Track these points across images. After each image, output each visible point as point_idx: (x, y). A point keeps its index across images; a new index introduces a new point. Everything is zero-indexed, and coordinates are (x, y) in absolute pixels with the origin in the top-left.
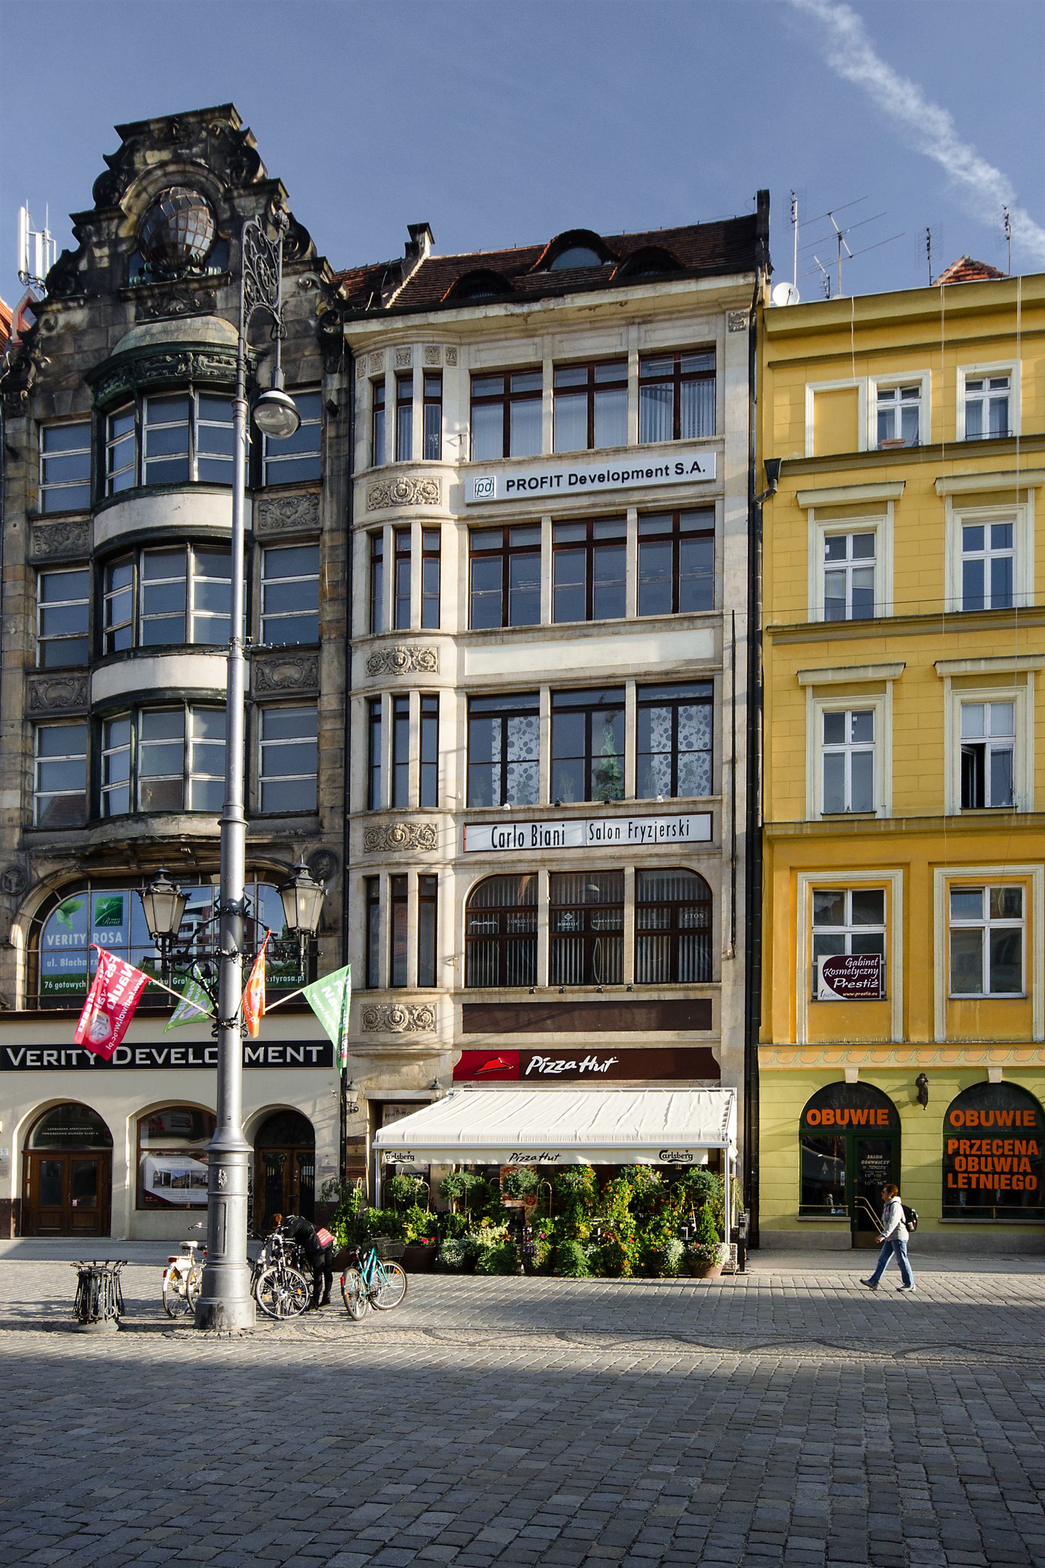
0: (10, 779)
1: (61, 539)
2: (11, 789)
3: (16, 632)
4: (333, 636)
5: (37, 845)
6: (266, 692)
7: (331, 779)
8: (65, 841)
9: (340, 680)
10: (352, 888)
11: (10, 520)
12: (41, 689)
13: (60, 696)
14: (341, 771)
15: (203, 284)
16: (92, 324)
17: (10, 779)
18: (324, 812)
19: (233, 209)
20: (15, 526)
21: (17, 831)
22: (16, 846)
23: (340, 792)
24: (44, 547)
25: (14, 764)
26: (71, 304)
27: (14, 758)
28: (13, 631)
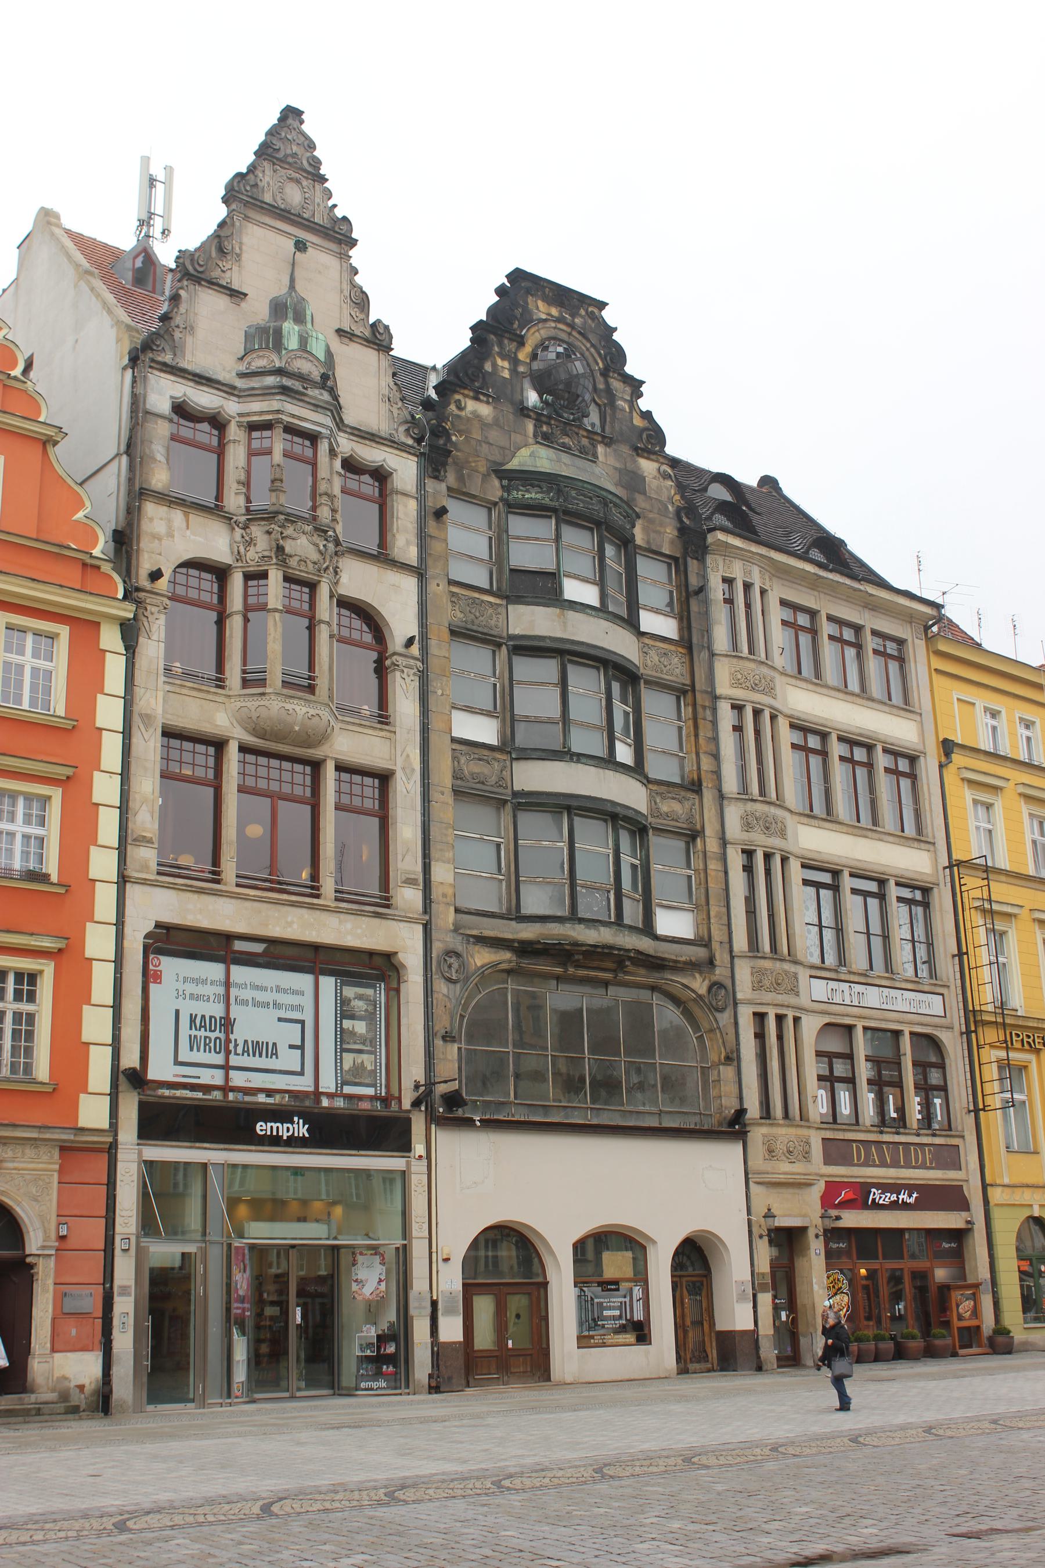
0: (441, 850)
1: (478, 614)
2: (444, 862)
3: (442, 695)
4: (710, 786)
5: (465, 927)
6: (665, 822)
7: (718, 916)
8: (493, 929)
9: (718, 827)
10: (741, 1021)
11: (434, 578)
12: (463, 760)
13: (483, 773)
14: (724, 910)
15: (591, 436)
16: (496, 423)
17: (441, 850)
18: (715, 945)
19: (607, 384)
20: (438, 585)
21: (452, 909)
22: (452, 927)
23: (726, 928)
24: (460, 615)
25: (446, 835)
26: (482, 397)
27: (446, 828)
28: (440, 692)
